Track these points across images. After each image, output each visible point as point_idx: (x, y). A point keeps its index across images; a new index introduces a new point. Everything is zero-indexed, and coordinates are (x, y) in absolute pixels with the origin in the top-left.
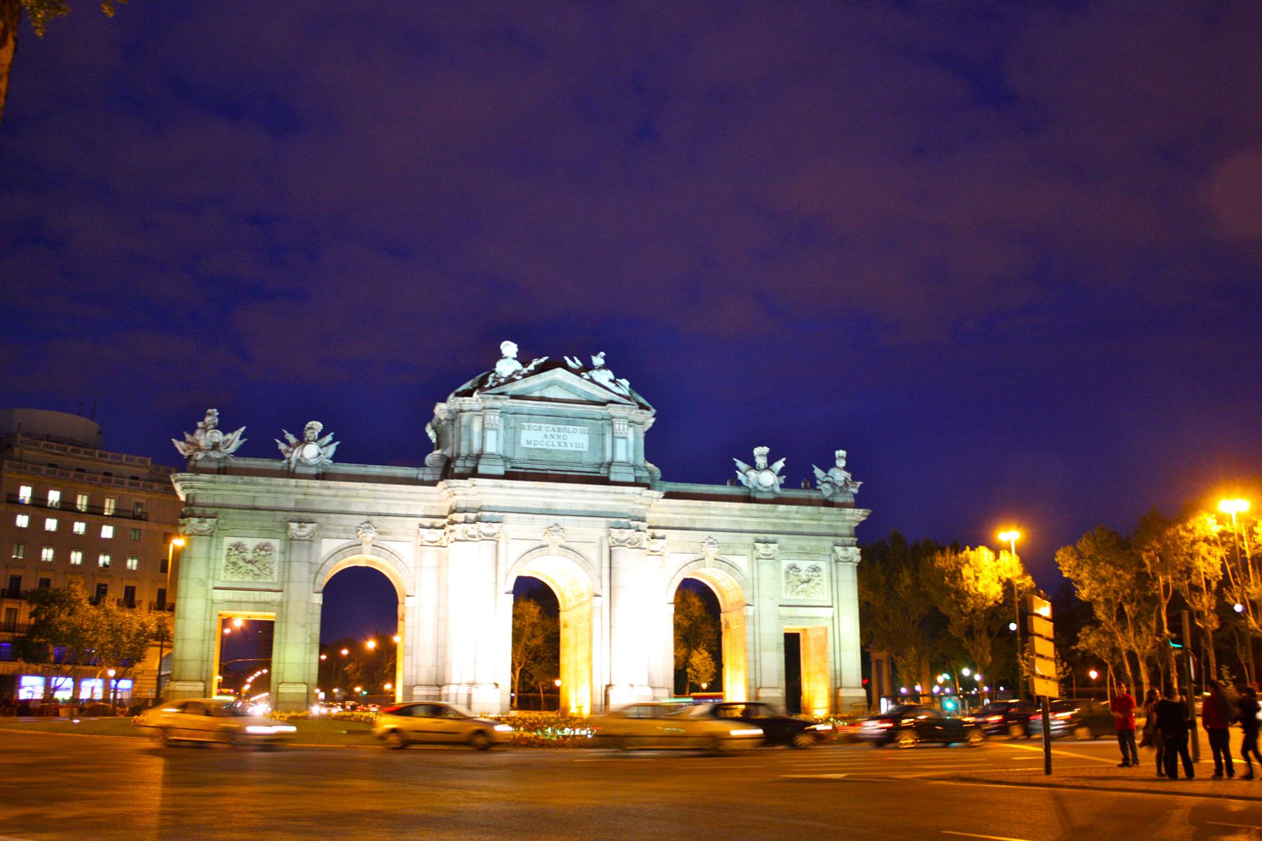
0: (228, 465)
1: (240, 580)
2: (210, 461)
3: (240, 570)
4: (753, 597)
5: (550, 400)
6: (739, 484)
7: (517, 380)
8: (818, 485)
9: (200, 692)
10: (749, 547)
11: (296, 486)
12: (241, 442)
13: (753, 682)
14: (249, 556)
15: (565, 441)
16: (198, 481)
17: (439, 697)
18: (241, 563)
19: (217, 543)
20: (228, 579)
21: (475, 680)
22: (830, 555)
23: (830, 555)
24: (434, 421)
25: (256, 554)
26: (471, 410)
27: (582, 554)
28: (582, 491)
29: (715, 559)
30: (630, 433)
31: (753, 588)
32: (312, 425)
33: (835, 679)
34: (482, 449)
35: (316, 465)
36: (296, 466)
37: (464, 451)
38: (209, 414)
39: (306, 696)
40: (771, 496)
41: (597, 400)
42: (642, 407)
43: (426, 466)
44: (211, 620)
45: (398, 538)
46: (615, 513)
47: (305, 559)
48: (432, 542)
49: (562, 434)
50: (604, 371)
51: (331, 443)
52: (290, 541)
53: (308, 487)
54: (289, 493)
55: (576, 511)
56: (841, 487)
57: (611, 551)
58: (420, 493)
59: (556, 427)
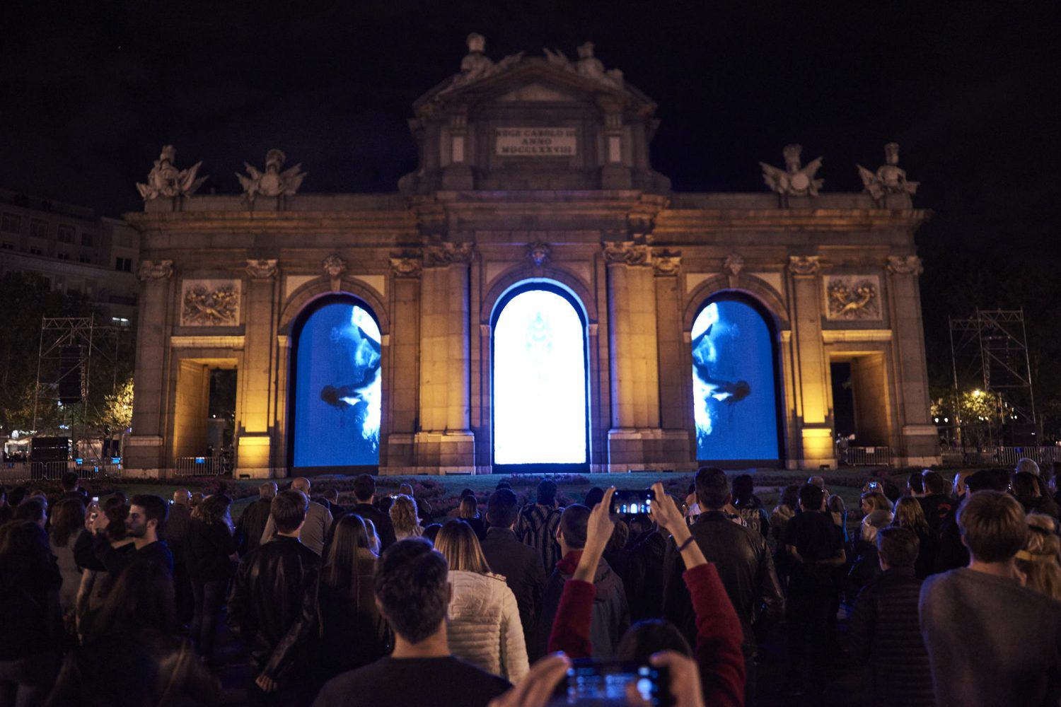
1: (201, 325)
10: (782, 262)
11: (252, 220)
20: (188, 324)
35: (278, 197)
48: (406, 273)
49: (544, 138)
51: (298, 174)
59: (537, 130)
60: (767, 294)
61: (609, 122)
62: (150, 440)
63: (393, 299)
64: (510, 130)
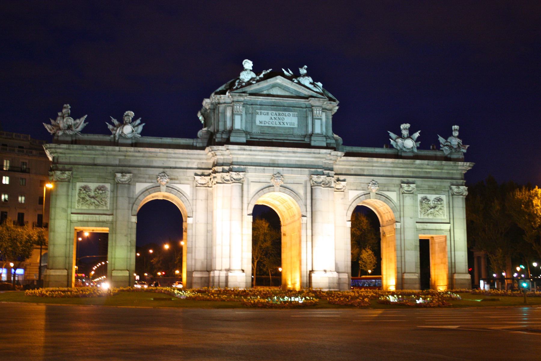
0: (77, 139)
1: (87, 208)
2: (66, 136)
3: (87, 202)
4: (400, 217)
6: (391, 147)
7: (253, 84)
8: (441, 147)
9: (65, 276)
10: (397, 186)
11: (119, 151)
12: (85, 125)
13: (400, 269)
14: (92, 194)
15: (283, 121)
16: (60, 148)
17: (209, 277)
18: (88, 198)
19: (72, 185)
20: (80, 208)
21: (230, 268)
22: (448, 191)
23: (448, 191)
24: (203, 110)
25: (96, 193)
26: (225, 103)
27: (294, 190)
28: (294, 152)
29: (376, 194)
31: (400, 211)
32: (128, 113)
33: (452, 268)
34: (232, 127)
35: (131, 138)
36: (119, 138)
37: (221, 128)
38: (65, 108)
39: (128, 278)
40: (411, 154)
41: (303, 95)
42: (330, 99)
43: (198, 138)
44: (70, 233)
45: (182, 182)
46: (315, 165)
47: (126, 195)
48: (203, 184)
49: (281, 117)
50: (307, 77)
51: (139, 124)
52: (117, 185)
53: (127, 151)
54: (115, 155)
55: (290, 164)
56: (455, 149)
57: (312, 189)
58: (194, 154)
59: (277, 113)
60: (390, 203)
61: (315, 112)
62: (62, 272)
63: (195, 198)
64: (263, 111)
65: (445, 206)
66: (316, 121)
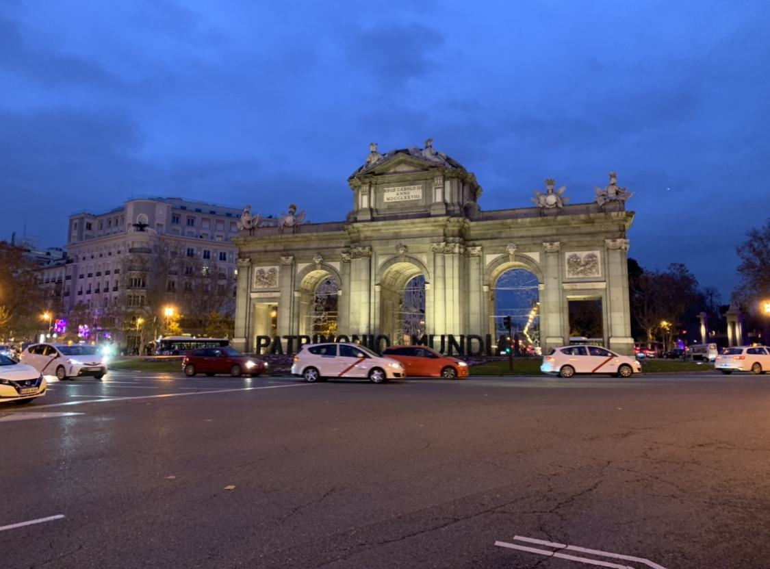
5: (399, 173)
11: (282, 238)
14: (266, 276)
18: (262, 279)
28: (413, 223)
29: (516, 256)
30: (448, 184)
40: (555, 211)
47: (289, 274)
49: (407, 191)
52: (284, 266)
59: (403, 188)
65: (599, 263)
66: (437, 190)
